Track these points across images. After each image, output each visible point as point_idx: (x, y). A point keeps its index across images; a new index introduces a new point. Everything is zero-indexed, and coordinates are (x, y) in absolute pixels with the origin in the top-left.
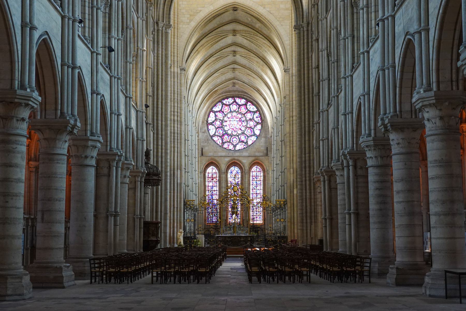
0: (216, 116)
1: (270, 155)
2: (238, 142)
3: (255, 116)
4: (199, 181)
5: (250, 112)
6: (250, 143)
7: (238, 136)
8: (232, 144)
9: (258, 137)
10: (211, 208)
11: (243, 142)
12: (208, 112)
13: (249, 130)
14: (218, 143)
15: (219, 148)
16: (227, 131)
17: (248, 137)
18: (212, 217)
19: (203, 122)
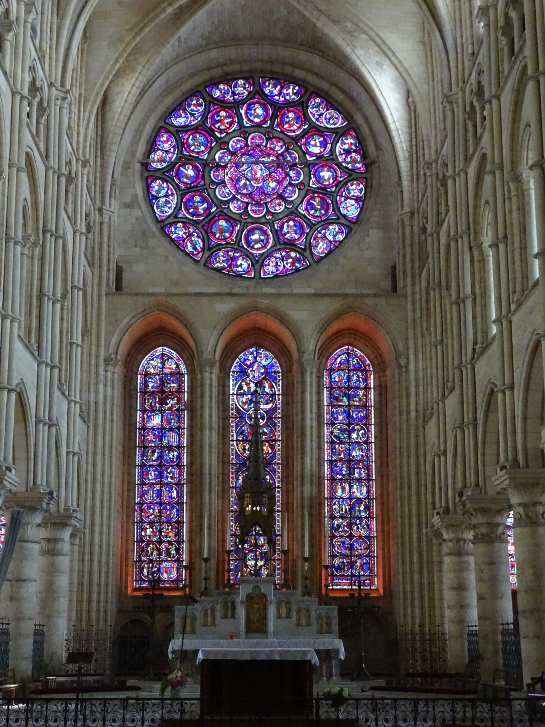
0: (181, 145)
1: (409, 289)
2: (269, 247)
3: (338, 149)
4: (101, 399)
5: (320, 131)
6: (321, 248)
7: (270, 223)
8: (247, 256)
9: (355, 228)
10: (151, 524)
11: (291, 245)
12: (149, 128)
13: (316, 203)
14: (190, 249)
15: (189, 267)
16: (227, 202)
17: (311, 226)
18: (160, 562)
19: (127, 166)
